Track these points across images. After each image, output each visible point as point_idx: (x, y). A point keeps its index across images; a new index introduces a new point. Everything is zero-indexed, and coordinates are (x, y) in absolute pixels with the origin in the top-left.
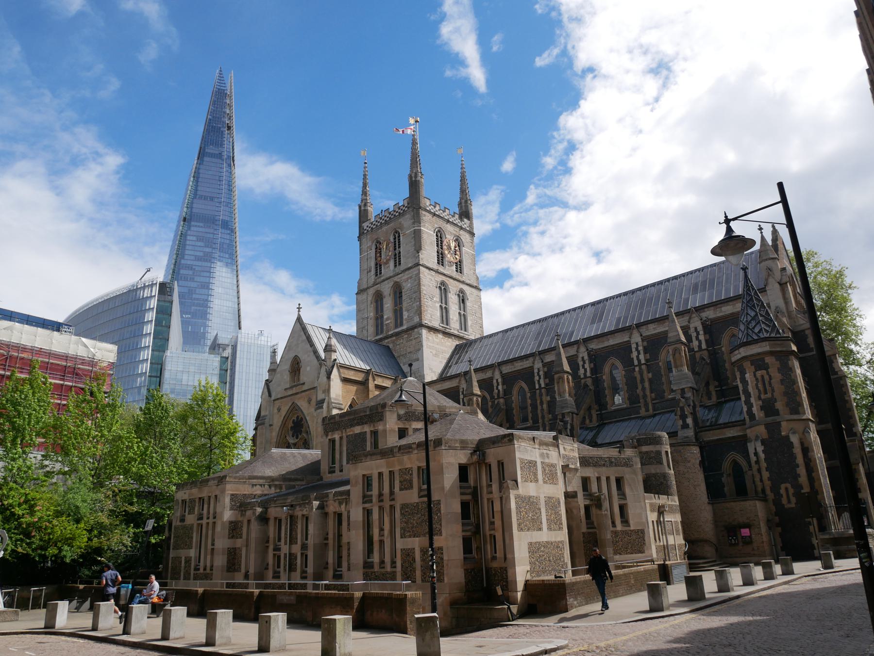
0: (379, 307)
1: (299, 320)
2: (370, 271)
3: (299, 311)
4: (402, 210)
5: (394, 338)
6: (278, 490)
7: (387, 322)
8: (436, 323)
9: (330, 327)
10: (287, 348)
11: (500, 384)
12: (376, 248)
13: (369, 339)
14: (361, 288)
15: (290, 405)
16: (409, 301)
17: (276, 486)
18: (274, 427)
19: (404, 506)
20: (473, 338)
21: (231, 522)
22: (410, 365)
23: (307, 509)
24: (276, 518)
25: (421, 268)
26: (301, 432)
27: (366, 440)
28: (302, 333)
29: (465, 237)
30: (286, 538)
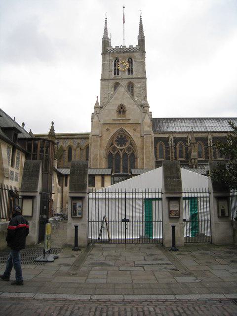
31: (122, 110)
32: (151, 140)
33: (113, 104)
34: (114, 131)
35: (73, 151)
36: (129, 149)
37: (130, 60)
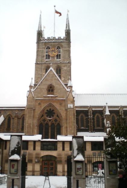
2: (44, 57)
18: (36, 111)
31: (51, 89)
32: (73, 112)
33: (44, 84)
34: (44, 106)
35: (12, 120)
36: (56, 120)
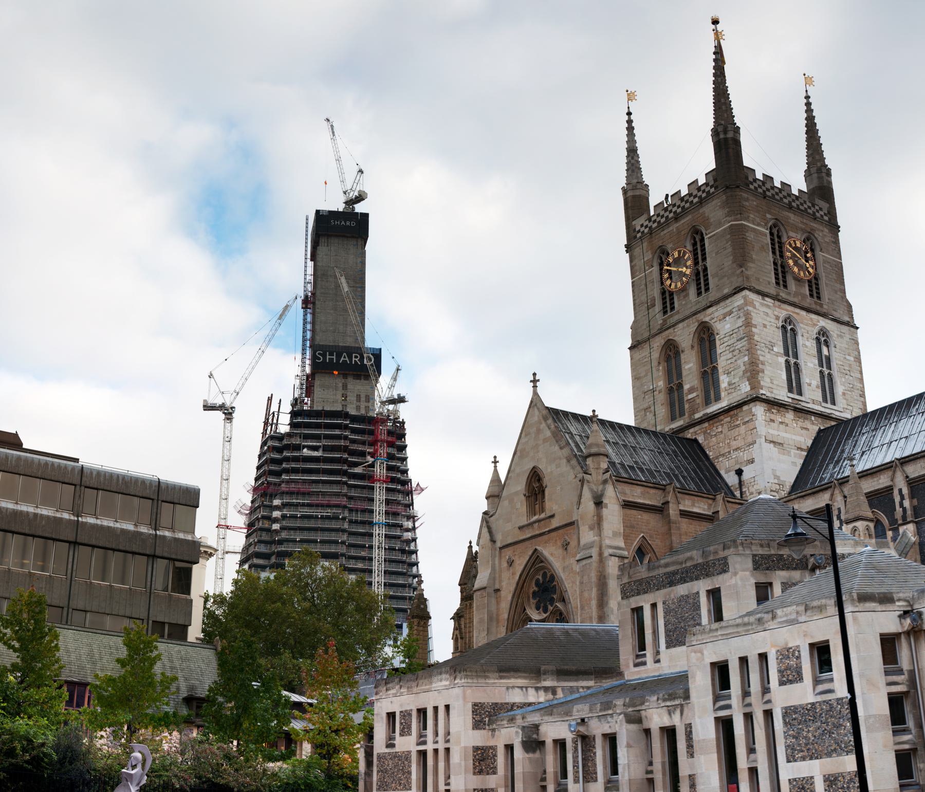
0: (674, 370)
1: (536, 402)
2: (654, 305)
3: (535, 387)
4: (704, 191)
5: (706, 425)
6: (550, 696)
7: (690, 396)
8: (783, 395)
9: (594, 411)
10: (518, 453)
11: (906, 497)
12: (661, 265)
13: (659, 428)
14: (639, 338)
15: (530, 553)
16: (730, 355)
17: (546, 689)
18: (503, 593)
19: (788, 712)
20: (849, 417)
21: (476, 749)
22: (739, 472)
23: (610, 724)
24: (555, 741)
25: (746, 292)
26: (552, 601)
27: (699, 607)
28: (543, 425)
29: (822, 234)
30: (576, 772)
37: (698, 238)
